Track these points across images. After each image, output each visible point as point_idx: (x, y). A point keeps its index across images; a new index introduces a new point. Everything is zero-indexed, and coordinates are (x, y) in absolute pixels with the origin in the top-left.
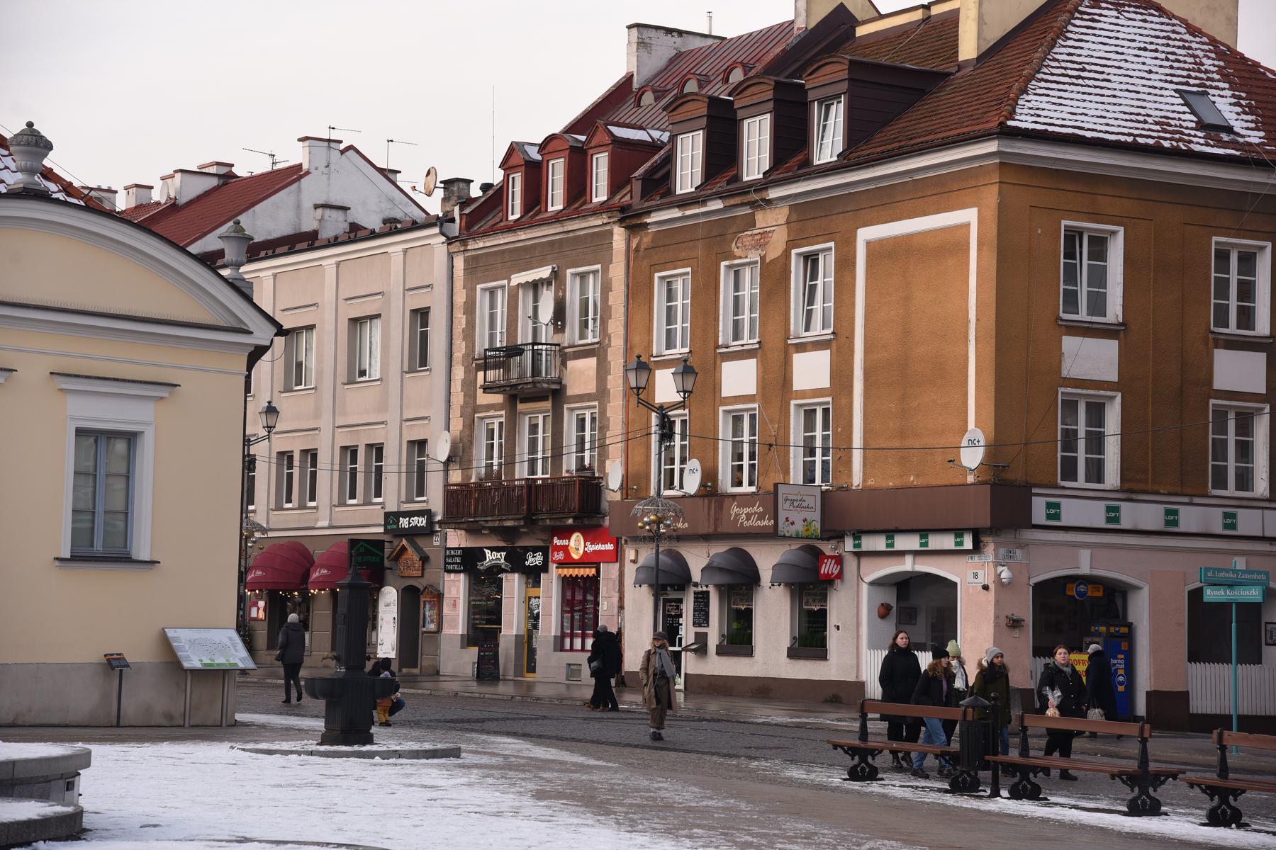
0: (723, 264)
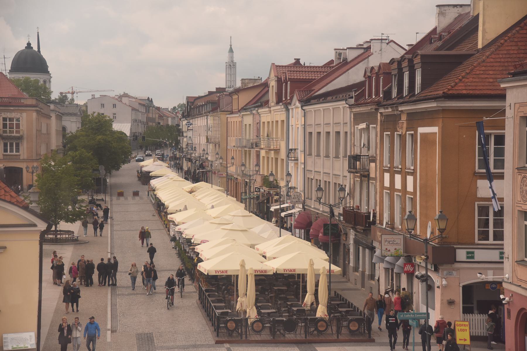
0: (396, 133)
